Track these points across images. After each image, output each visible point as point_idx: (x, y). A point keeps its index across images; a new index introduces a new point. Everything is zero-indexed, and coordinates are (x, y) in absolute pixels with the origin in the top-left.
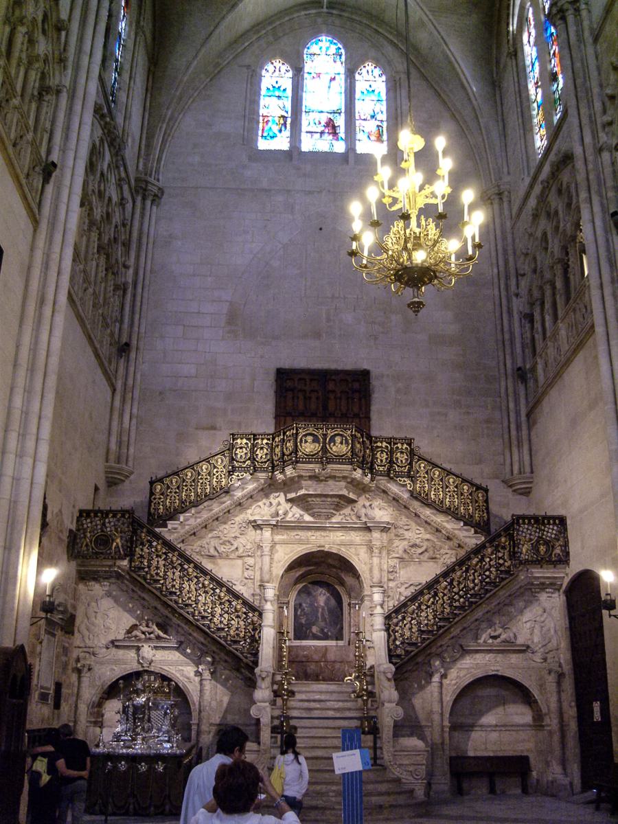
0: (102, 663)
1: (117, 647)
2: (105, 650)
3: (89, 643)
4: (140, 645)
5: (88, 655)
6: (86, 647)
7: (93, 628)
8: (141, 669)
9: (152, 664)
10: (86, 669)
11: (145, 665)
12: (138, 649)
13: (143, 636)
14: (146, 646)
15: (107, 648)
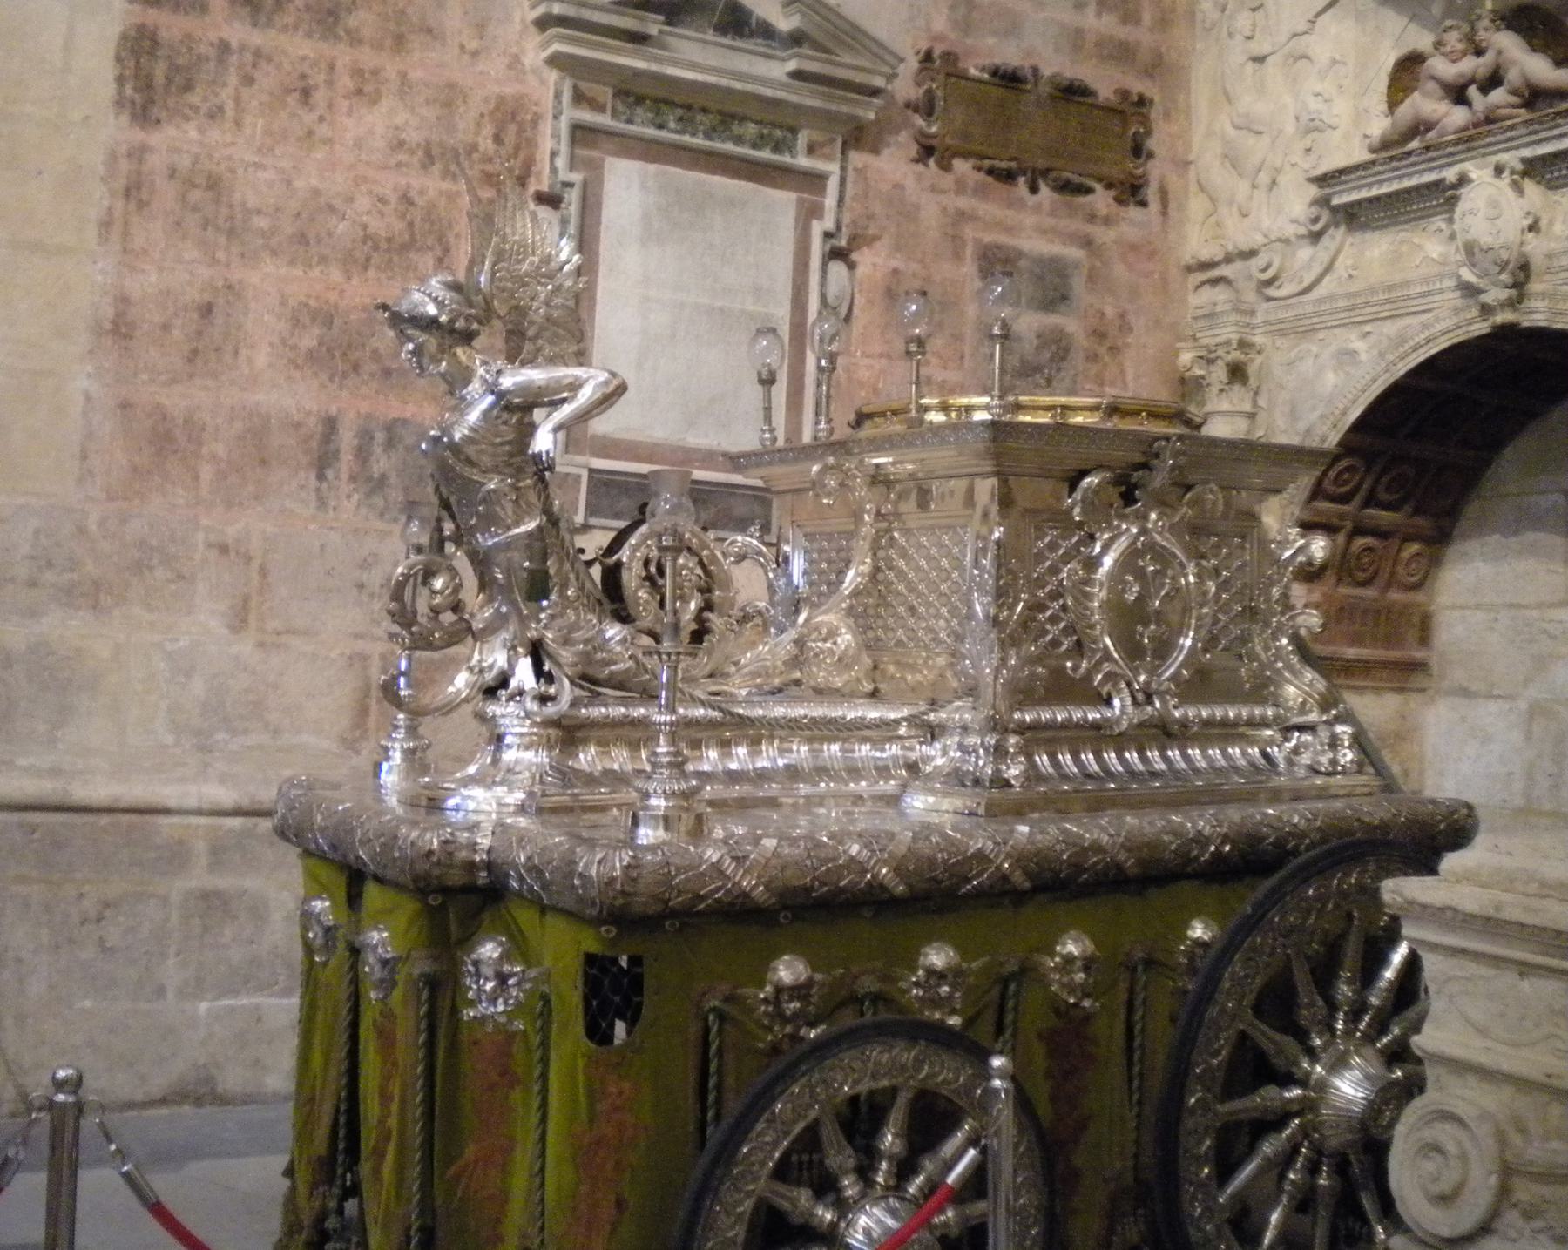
0: (1300, 330)
1: (1353, 217)
2: (1305, 252)
3: (1239, 235)
4: (1450, 175)
5: (1220, 295)
6: (1228, 259)
7: (1251, 140)
8: (1480, 328)
9: (1535, 286)
10: (1219, 373)
11: (1488, 298)
12: (1444, 197)
13: (1458, 116)
14: (1479, 171)
15: (1316, 237)
